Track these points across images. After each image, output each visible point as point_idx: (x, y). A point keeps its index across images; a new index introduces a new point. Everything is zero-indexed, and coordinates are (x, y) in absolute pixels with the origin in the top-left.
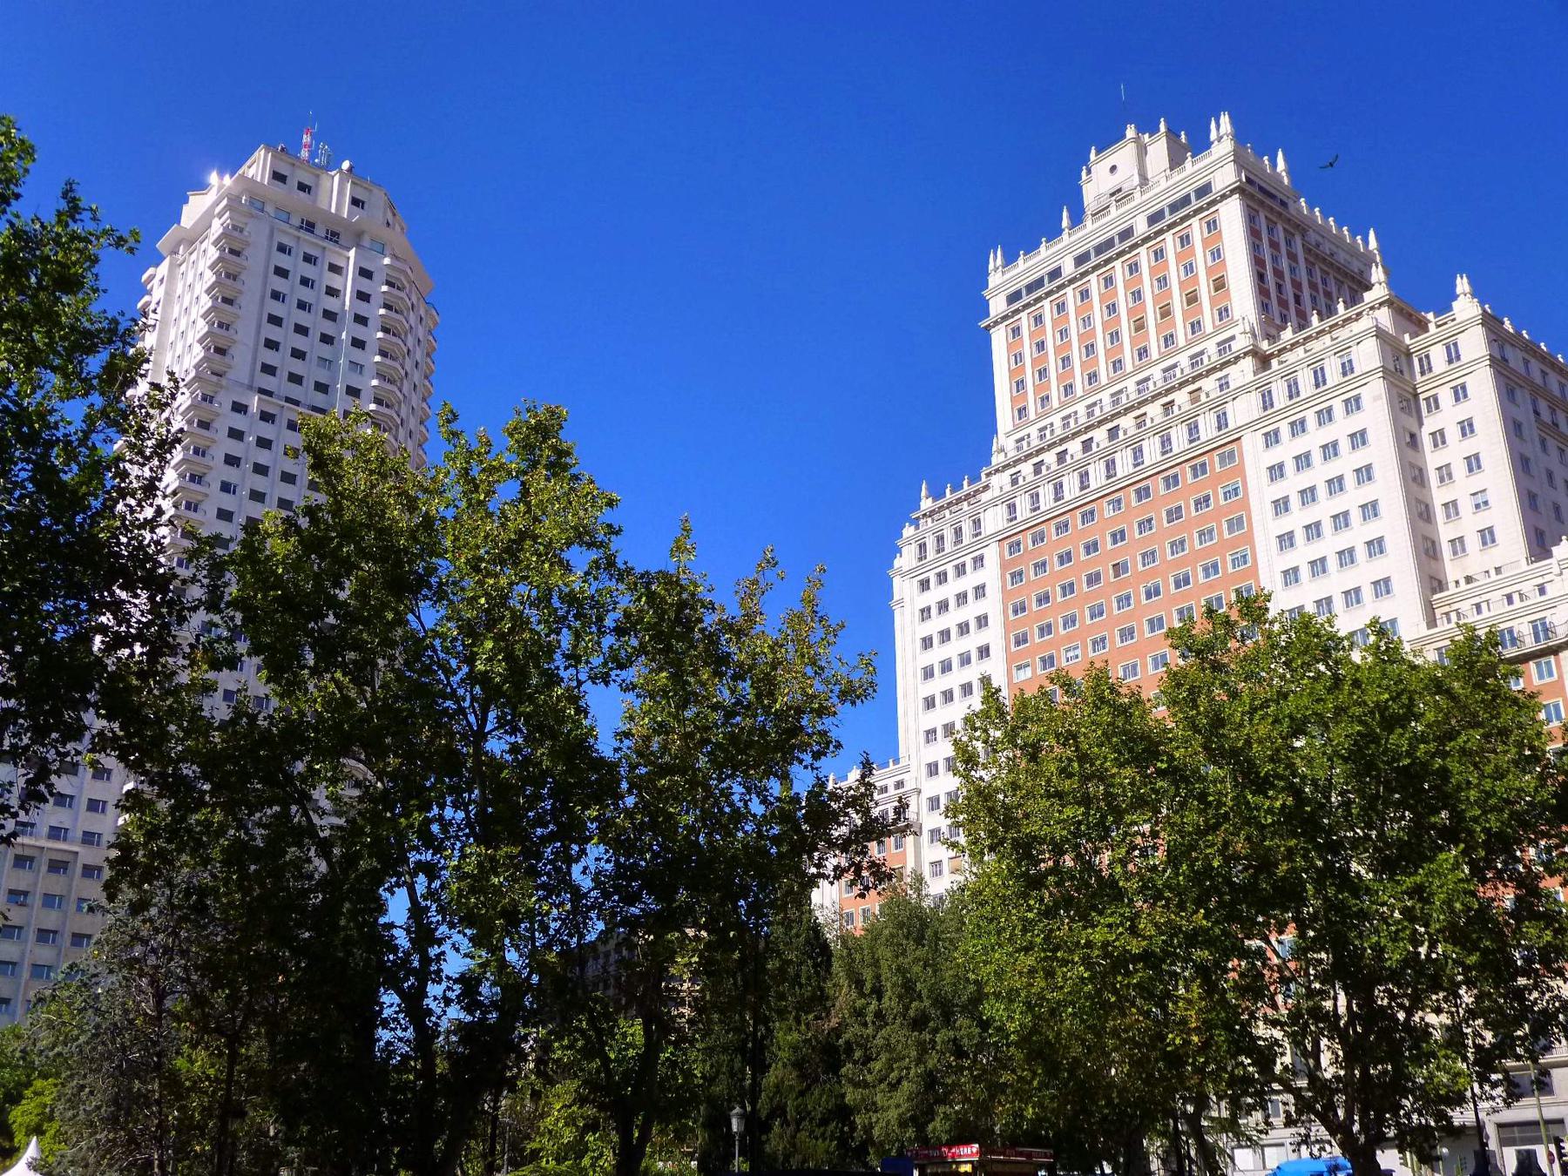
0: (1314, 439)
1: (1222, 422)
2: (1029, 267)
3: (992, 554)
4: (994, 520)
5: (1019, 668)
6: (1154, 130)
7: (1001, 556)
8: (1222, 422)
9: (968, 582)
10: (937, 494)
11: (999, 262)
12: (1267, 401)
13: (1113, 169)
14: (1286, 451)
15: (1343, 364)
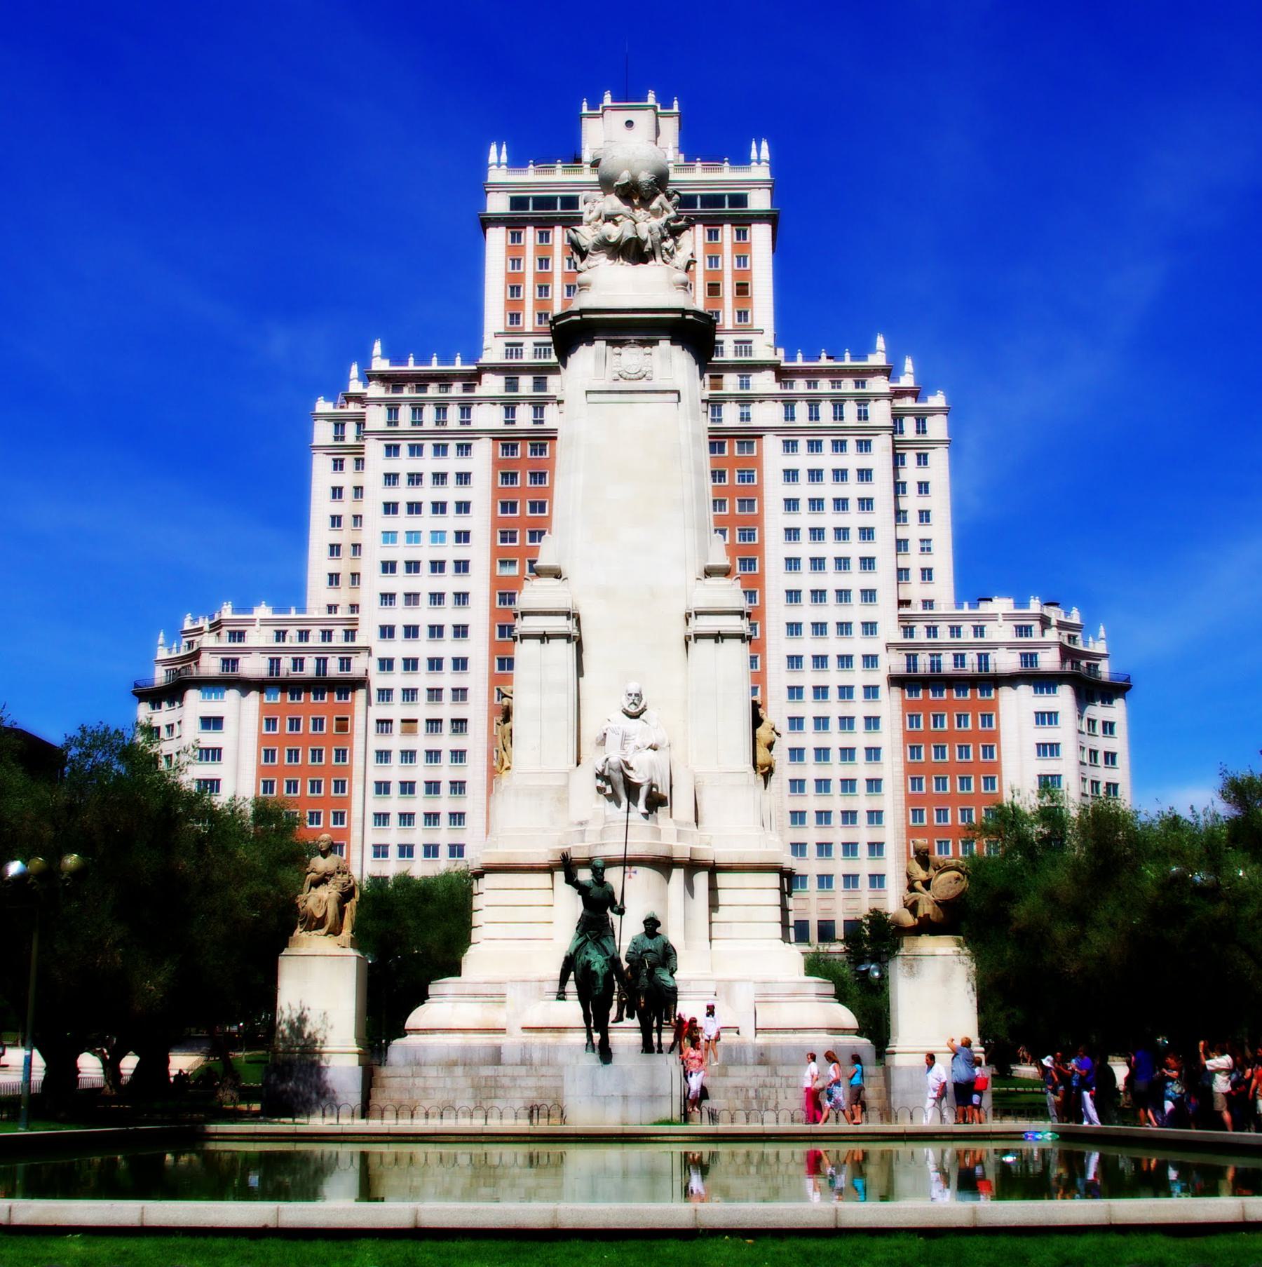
0: (827, 460)
1: (745, 417)
2: (532, 177)
3: (483, 450)
4: (488, 417)
5: (503, 563)
6: (667, 104)
7: (495, 454)
8: (745, 417)
9: (452, 463)
10: (397, 359)
11: (504, 158)
12: (790, 416)
13: (629, 124)
14: (803, 460)
15: (860, 411)
